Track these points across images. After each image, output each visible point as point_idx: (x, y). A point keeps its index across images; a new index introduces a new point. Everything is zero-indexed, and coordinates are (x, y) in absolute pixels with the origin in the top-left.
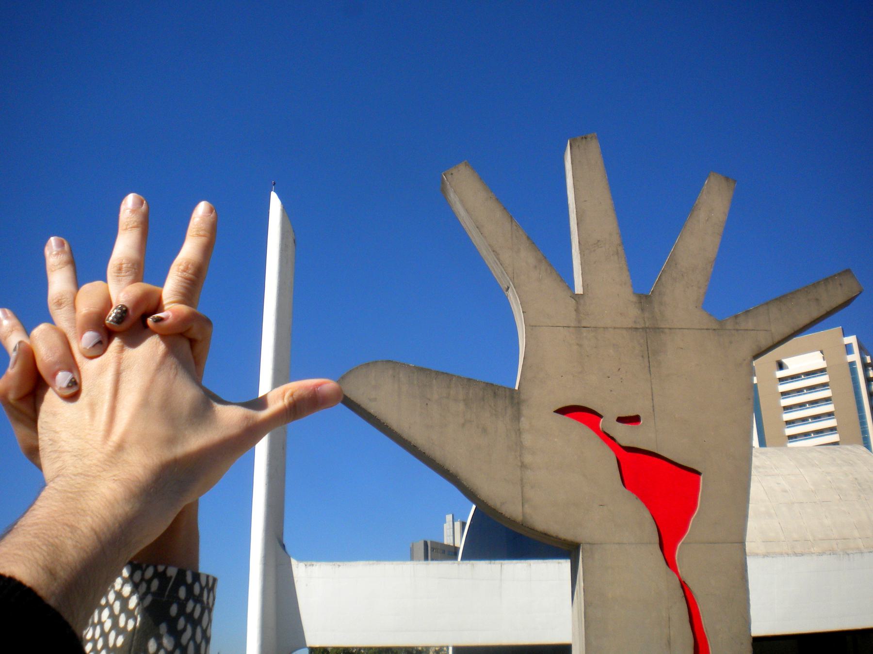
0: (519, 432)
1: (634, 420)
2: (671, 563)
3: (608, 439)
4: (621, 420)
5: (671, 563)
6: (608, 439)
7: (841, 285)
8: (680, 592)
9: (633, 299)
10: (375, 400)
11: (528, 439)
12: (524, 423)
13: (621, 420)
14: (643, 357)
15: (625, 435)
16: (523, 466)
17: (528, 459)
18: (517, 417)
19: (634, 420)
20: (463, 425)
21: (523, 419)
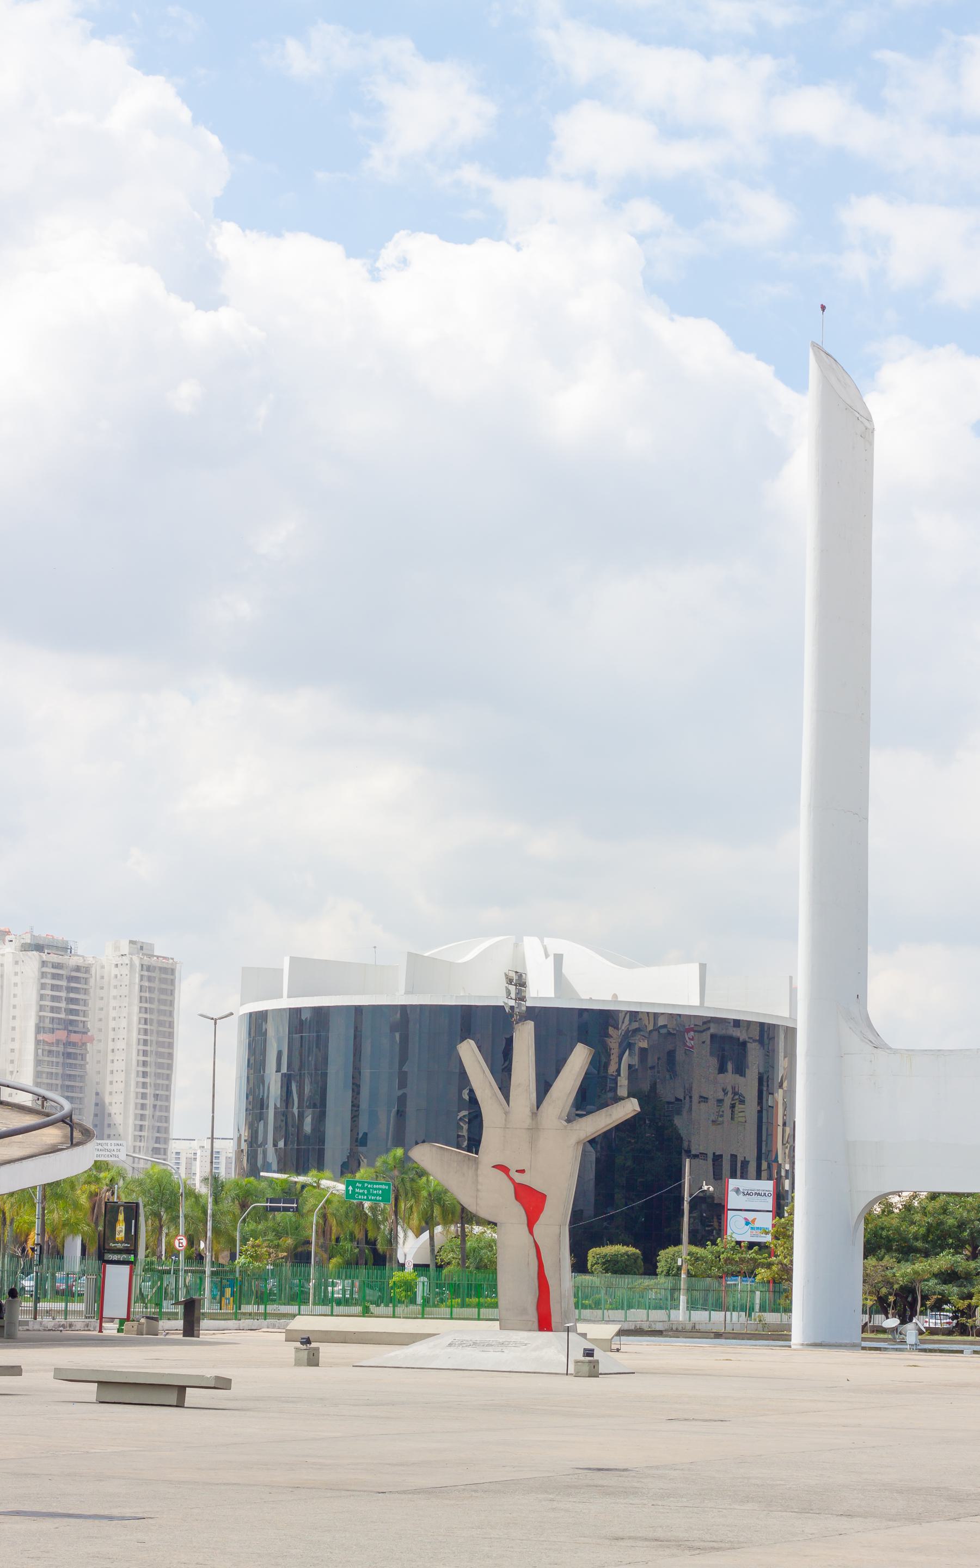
0: (477, 1175)
1: (522, 1171)
2: (531, 1232)
3: (511, 1179)
4: (517, 1171)
5: (531, 1232)
6: (511, 1179)
7: (624, 1107)
8: (533, 1244)
9: (530, 1114)
10: (423, 1161)
11: (480, 1179)
12: (479, 1172)
13: (517, 1171)
14: (530, 1143)
15: (519, 1178)
16: (478, 1190)
17: (480, 1187)
18: (477, 1169)
19: (522, 1171)
20: (456, 1172)
21: (479, 1170)
